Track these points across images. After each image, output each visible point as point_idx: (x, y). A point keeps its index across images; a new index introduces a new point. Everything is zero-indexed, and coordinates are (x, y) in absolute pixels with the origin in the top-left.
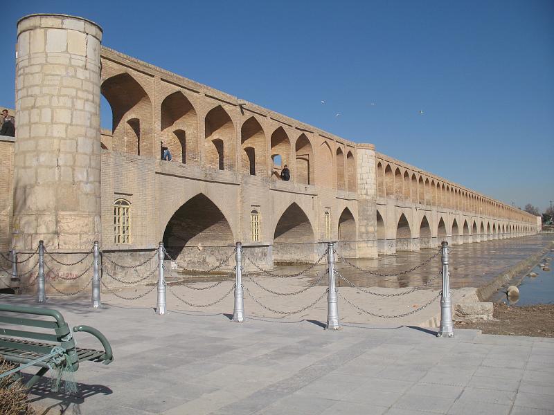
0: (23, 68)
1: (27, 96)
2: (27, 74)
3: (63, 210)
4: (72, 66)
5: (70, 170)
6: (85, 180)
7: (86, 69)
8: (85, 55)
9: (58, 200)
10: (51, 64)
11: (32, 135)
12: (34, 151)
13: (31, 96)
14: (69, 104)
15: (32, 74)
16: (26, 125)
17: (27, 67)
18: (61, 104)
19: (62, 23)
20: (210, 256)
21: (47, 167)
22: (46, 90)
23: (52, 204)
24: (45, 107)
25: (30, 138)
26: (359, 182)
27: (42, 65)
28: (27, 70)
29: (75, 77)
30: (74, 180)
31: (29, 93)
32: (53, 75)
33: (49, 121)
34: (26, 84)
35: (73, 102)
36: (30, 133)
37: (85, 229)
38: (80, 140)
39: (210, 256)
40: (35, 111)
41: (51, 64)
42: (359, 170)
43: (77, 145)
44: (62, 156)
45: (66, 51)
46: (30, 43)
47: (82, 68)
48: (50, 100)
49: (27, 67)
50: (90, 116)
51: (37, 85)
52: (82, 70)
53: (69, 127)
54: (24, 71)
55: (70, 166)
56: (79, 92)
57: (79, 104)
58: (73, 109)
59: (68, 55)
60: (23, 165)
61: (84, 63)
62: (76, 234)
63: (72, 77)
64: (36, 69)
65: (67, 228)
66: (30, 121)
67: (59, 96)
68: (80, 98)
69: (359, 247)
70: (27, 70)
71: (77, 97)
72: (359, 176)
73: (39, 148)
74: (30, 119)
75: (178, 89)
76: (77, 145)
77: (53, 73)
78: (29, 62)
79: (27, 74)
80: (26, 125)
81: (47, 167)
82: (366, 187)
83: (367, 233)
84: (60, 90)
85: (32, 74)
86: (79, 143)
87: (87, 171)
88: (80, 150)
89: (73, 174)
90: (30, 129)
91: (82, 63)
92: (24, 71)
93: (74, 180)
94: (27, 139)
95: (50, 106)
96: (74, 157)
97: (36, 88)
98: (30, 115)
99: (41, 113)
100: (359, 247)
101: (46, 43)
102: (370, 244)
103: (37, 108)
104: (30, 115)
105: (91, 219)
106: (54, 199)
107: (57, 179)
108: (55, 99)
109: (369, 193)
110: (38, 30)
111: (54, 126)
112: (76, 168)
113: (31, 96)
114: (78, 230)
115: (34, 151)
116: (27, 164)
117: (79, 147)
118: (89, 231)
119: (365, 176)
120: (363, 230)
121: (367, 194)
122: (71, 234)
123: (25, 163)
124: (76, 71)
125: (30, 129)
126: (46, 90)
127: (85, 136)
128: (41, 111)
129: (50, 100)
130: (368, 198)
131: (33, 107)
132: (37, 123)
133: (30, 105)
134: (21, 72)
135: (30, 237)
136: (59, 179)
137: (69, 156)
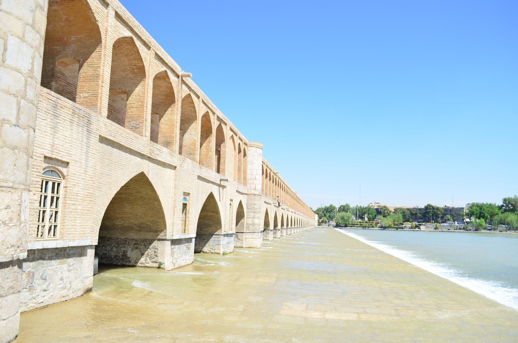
6: (14, 121)
20: (132, 250)
39: (132, 250)
50: (34, 6)
69: (245, 238)
76: (5, 50)
82: (256, 182)
83: (253, 224)
86: (10, 47)
87: (19, 103)
100: (245, 238)
102: (255, 235)
105: (16, 196)
109: (257, 188)
117: (8, 54)
118: (11, 219)
120: (250, 221)
121: (255, 189)
127: (22, 39)
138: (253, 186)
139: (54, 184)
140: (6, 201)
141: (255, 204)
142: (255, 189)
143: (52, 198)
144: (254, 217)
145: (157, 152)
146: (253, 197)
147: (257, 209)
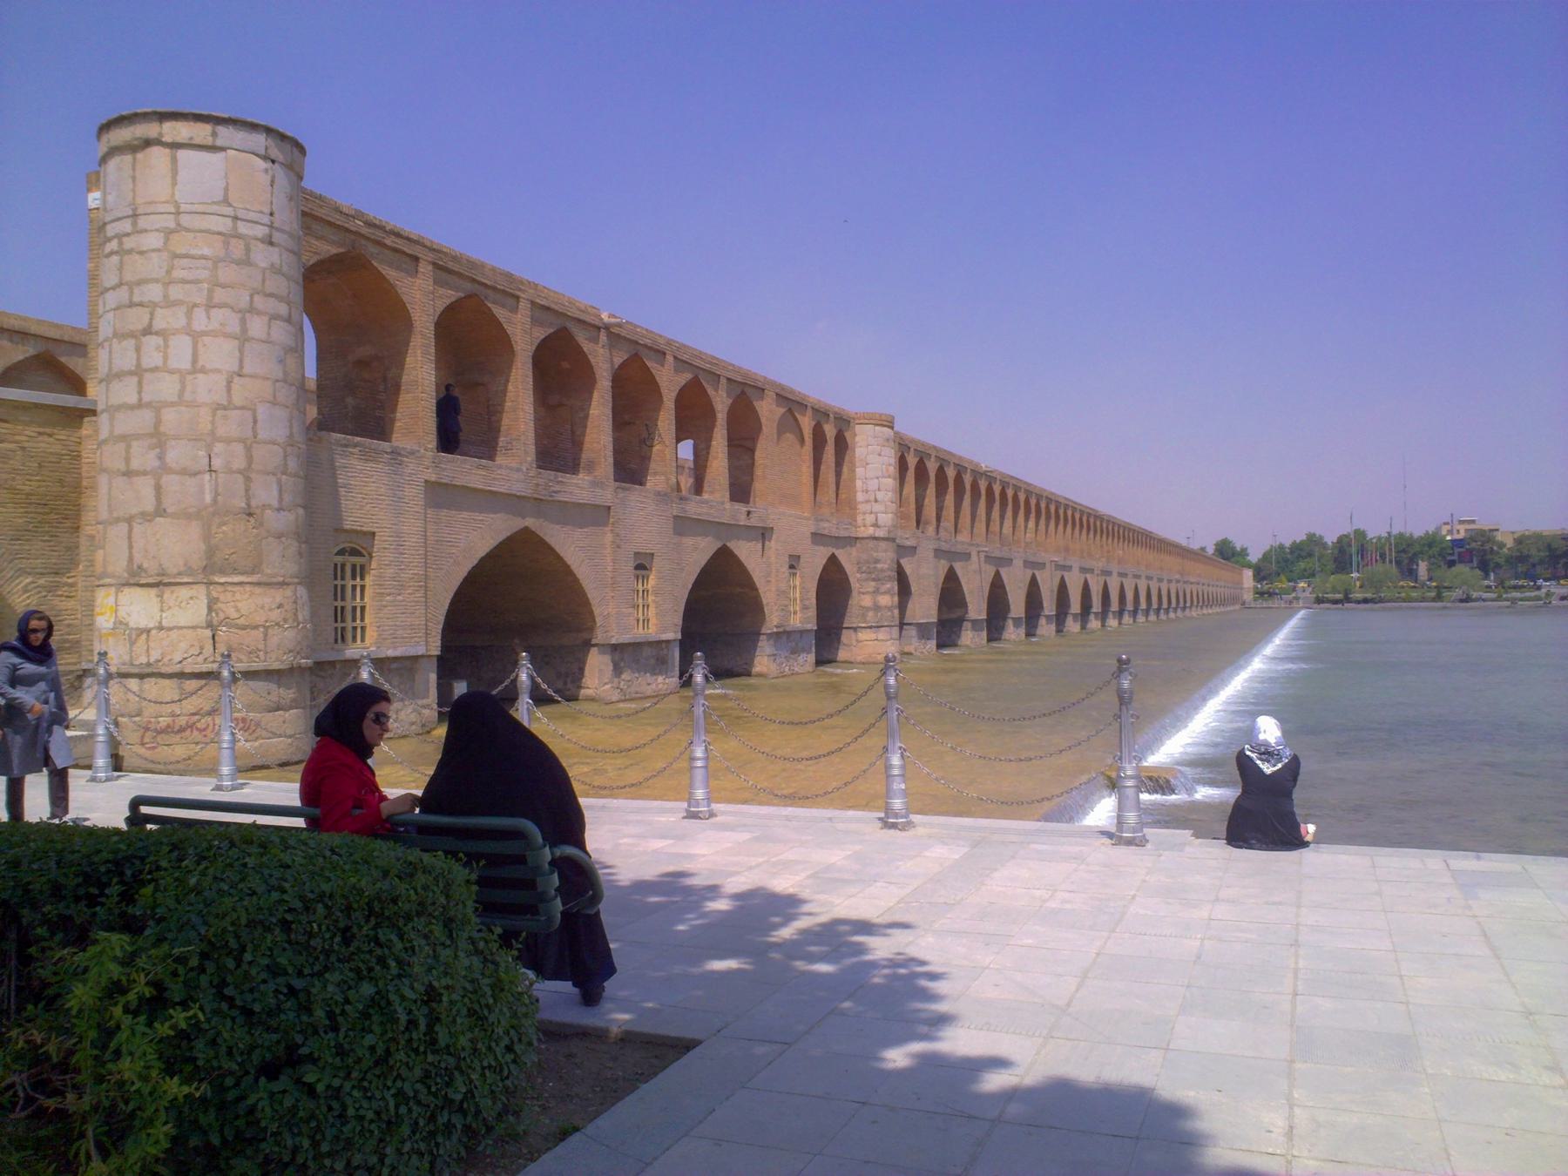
0: (120, 237)
1: (132, 305)
2: (130, 252)
3: (222, 572)
4: (239, 236)
5: (240, 478)
6: (275, 504)
7: (271, 244)
8: (267, 210)
9: (211, 552)
10: (188, 230)
11: (146, 398)
12: (151, 435)
13: (141, 305)
14: (234, 325)
15: (141, 253)
16: (131, 373)
17: (128, 235)
18: (214, 325)
19: (214, 134)
21: (184, 472)
22: (176, 292)
23: (197, 561)
24: (176, 332)
25: (140, 405)
26: (860, 497)
27: (169, 233)
28: (129, 243)
29: (246, 262)
30: (249, 505)
31: (136, 299)
32: (193, 257)
33: (185, 364)
34: (128, 277)
35: (243, 321)
36: (140, 393)
37: (276, 615)
38: (262, 411)
40: (152, 342)
41: (188, 230)
42: (859, 471)
43: (255, 421)
44: (219, 447)
45: (226, 201)
46: (134, 178)
47: (262, 241)
48: (189, 314)
49: (128, 235)
51: (157, 281)
52: (261, 246)
53: (236, 379)
54: (121, 243)
55: (240, 472)
56: (256, 298)
57: (257, 327)
58: (243, 338)
59: (228, 211)
60: (122, 467)
61: (266, 230)
62: (256, 627)
63: (238, 263)
64: (153, 241)
65: (234, 615)
66: (138, 365)
67: (210, 306)
68: (259, 313)
70: (129, 243)
71: (252, 310)
72: (859, 483)
73: (162, 429)
74: (138, 359)
75: (468, 286)
76: (255, 421)
77: (193, 252)
78: (134, 224)
79: (130, 252)
80: (131, 373)
81: (184, 472)
84: (210, 291)
85: (141, 253)
86: (260, 417)
87: (279, 483)
88: (262, 435)
89: (247, 491)
90: (140, 383)
91: (260, 231)
92: (121, 243)
93: (249, 505)
94: (132, 408)
95: (188, 331)
96: (248, 449)
97: (150, 286)
98: (138, 349)
99: (166, 346)
101: (174, 183)
102: (882, 634)
103: (157, 333)
104: (138, 349)
106: (203, 547)
107: (208, 498)
108: (200, 314)
109: (880, 522)
110: (155, 151)
111: (200, 376)
112: (253, 476)
113: (141, 305)
114: (259, 618)
115: (151, 435)
116: (135, 464)
117: (259, 424)
119: (873, 484)
121: (876, 525)
122: (244, 628)
123: (127, 460)
124: (248, 250)
125: (140, 383)
126: (176, 292)
127: (274, 403)
128: (166, 341)
129: (189, 314)
130: (880, 533)
131: (148, 331)
132: (155, 369)
133: (140, 327)
134: (113, 245)
135: (144, 636)
136: (215, 501)
137: (239, 449)
138: (870, 519)
139: (354, 566)
140: (278, 600)
141: (877, 561)
142: (876, 525)
143: (354, 587)
144: (876, 591)
145: (557, 488)
146: (871, 544)
147: (882, 570)
